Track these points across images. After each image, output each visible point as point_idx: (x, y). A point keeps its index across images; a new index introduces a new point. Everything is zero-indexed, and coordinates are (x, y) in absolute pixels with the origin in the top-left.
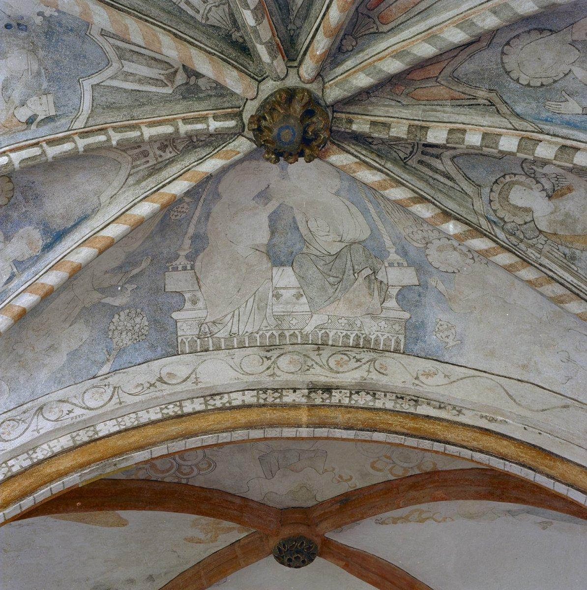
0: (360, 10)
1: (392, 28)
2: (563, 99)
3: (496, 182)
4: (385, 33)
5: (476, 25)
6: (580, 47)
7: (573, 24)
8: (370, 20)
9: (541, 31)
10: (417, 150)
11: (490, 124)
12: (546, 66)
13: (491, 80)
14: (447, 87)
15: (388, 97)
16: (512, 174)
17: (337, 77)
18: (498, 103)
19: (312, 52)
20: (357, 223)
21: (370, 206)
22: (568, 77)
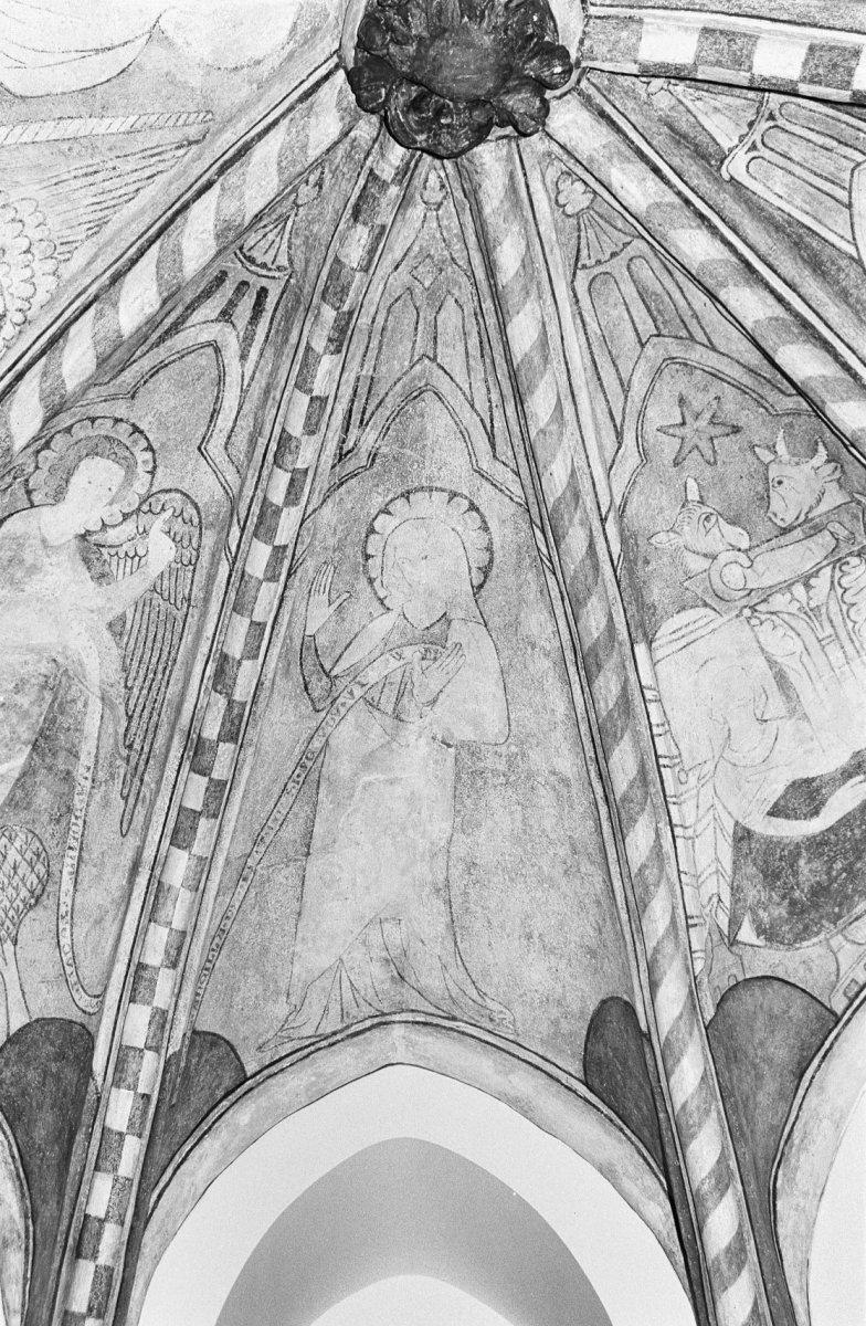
0: (639, 243)
1: (577, 301)
2: (334, 596)
3: (136, 429)
4: (572, 282)
5: (576, 509)
6: (436, 630)
7: (486, 626)
8: (607, 256)
9: (486, 571)
10: (247, 269)
11: (320, 470)
12: (408, 568)
13: (396, 459)
14: (405, 374)
15: (416, 248)
16: (155, 468)
17: (525, 175)
18: (342, 467)
19: (620, 153)
20: (47, 59)
21: (119, 125)
22: (377, 604)
